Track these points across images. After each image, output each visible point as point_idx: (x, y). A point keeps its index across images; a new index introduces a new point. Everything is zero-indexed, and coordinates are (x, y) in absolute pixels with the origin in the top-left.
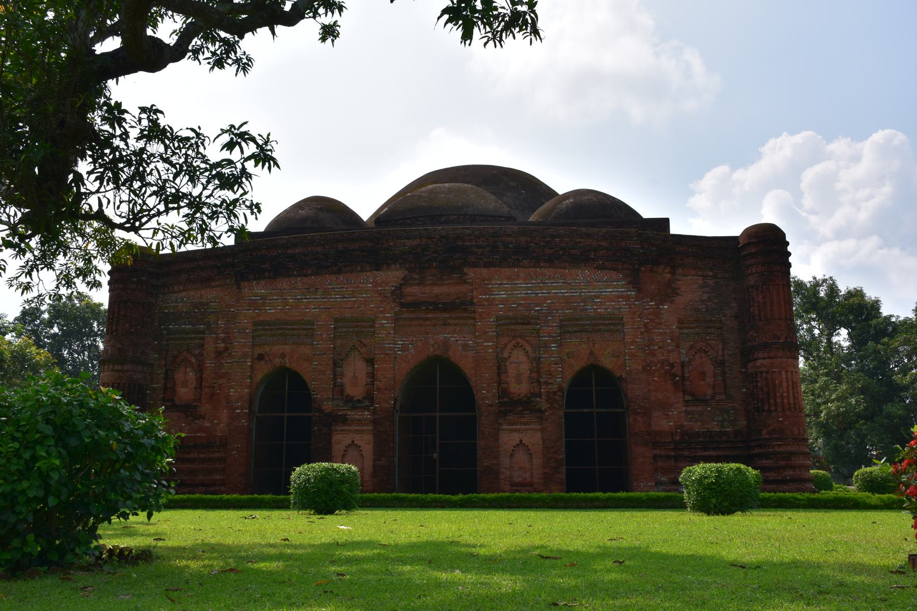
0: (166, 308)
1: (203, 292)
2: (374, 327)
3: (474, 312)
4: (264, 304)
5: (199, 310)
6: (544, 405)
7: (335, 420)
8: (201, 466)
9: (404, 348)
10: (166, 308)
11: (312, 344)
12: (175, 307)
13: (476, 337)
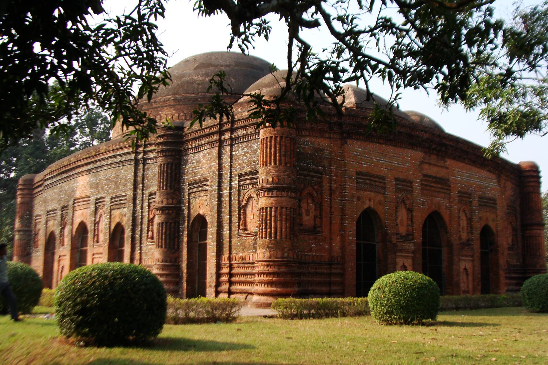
0: (298, 148)
1: (320, 140)
2: (412, 187)
3: (450, 186)
5: (318, 153)
9: (423, 204)
10: (298, 148)
11: (384, 194)
12: (304, 148)
13: (451, 202)
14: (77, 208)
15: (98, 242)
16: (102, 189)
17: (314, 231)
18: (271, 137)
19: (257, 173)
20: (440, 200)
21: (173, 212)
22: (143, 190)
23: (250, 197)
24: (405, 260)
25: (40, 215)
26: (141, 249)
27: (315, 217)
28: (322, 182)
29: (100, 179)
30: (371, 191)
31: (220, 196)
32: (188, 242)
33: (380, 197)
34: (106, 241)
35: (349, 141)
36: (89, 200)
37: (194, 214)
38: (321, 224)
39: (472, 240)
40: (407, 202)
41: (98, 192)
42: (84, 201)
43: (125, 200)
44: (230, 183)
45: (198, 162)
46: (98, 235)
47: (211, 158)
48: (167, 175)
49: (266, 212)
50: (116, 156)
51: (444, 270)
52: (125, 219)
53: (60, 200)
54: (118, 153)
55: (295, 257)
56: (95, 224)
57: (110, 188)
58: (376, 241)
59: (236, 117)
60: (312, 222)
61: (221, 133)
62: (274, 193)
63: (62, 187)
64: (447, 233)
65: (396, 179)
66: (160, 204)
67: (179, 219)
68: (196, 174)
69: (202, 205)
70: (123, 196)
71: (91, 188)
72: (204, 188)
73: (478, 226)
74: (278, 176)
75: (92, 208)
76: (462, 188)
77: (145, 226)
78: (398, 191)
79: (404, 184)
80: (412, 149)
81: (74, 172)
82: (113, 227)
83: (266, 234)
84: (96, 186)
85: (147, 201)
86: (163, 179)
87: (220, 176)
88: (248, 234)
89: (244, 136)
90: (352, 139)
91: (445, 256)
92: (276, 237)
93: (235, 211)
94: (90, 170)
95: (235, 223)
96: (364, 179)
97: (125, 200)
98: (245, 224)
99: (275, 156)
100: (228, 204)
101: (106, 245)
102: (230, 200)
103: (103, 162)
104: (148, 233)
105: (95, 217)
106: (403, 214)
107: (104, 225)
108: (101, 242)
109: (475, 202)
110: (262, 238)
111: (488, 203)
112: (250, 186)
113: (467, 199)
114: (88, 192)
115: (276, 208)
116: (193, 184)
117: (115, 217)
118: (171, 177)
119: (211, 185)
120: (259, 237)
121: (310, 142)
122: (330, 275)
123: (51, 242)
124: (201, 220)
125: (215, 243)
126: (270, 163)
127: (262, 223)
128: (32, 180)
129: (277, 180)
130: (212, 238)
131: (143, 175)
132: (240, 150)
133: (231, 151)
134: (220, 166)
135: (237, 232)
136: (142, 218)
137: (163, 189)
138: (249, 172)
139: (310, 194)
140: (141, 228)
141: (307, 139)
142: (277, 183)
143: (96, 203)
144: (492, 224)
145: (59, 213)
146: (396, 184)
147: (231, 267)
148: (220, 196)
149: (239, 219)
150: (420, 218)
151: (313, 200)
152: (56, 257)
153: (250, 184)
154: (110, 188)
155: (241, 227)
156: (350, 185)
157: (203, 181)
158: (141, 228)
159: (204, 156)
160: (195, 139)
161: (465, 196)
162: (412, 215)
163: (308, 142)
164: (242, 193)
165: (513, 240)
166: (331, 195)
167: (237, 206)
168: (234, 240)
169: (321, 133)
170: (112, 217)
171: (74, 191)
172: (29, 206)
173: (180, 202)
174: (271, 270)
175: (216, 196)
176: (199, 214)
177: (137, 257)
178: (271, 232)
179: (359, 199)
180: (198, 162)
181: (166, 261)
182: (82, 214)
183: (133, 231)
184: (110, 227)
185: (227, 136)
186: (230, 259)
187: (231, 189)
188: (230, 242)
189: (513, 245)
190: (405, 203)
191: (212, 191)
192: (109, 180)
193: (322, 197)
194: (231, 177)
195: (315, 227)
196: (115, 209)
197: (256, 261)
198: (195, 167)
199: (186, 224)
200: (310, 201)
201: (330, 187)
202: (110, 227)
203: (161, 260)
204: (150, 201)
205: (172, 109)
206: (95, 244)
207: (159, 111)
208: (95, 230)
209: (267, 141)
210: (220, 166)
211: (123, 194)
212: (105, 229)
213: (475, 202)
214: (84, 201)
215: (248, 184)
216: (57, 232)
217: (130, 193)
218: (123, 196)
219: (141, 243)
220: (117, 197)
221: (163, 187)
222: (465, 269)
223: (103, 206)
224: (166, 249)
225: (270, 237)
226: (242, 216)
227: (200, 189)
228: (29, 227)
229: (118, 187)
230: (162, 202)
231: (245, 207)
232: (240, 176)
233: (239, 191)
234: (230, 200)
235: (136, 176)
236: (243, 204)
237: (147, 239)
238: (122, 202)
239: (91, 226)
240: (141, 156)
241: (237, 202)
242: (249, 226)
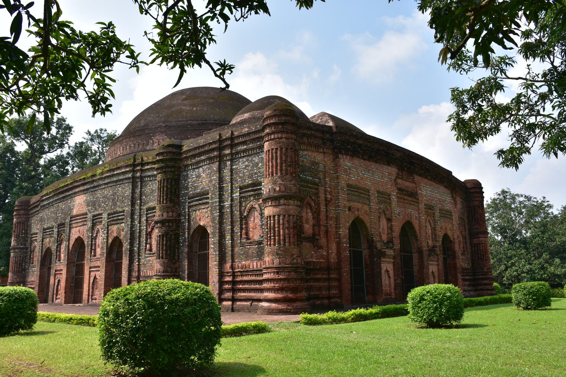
2: (390, 199)
3: (418, 199)
4: (350, 174)
6: (439, 252)
7: (382, 254)
8: (324, 284)
13: (419, 213)
14: (74, 225)
15: (95, 256)
16: (100, 206)
17: (313, 239)
18: (277, 149)
19: (260, 184)
20: (412, 211)
21: (173, 225)
22: (141, 205)
23: (252, 208)
24: (388, 265)
25: (36, 234)
26: (139, 261)
27: (314, 226)
28: (318, 193)
29: (98, 197)
30: (359, 202)
31: (221, 208)
32: (189, 253)
33: (366, 208)
34: (104, 255)
35: (340, 156)
36: (86, 217)
37: (194, 226)
38: (319, 232)
39: (436, 247)
40: (387, 213)
41: (96, 209)
42: (80, 219)
43: (122, 215)
44: (231, 195)
45: (197, 177)
46: (95, 250)
47: (211, 172)
48: (167, 190)
49: (274, 220)
50: (113, 176)
51: (415, 274)
52: (123, 233)
53: (57, 219)
54: (115, 173)
55: (303, 263)
56: (92, 239)
57: (107, 205)
58: (363, 248)
59: (236, 133)
60: (311, 231)
61: (221, 149)
62: (282, 201)
63: (58, 206)
64: (417, 240)
65: (378, 192)
66: (161, 217)
67: (179, 231)
68: (196, 188)
69: (204, 217)
70: (120, 212)
71: (88, 205)
72: (205, 201)
73: (441, 234)
74: (285, 186)
75: (89, 224)
76: (427, 201)
77: (143, 240)
78: (379, 203)
79: (384, 197)
80: (389, 166)
81: (71, 192)
82: (110, 241)
83: (275, 241)
84: (92, 204)
85: (145, 216)
86: (163, 194)
87: (221, 189)
88: (251, 243)
89: (244, 151)
90: (342, 154)
91: (415, 261)
92: (284, 244)
93: (237, 221)
94: (87, 189)
95: (237, 233)
96: (353, 191)
97: (122, 215)
98: (247, 234)
99: (281, 167)
100: (229, 215)
101: (104, 259)
102: (232, 212)
103: (101, 182)
104: (146, 246)
105: (92, 233)
106: (384, 222)
107: (101, 240)
108: (98, 255)
109: (437, 214)
110: (270, 245)
111: (446, 214)
112: (252, 198)
113: (431, 211)
114: (84, 210)
115: (284, 216)
116: (193, 198)
117: (113, 232)
118: (171, 191)
119: (212, 198)
120: (267, 245)
121: (310, 156)
122: (328, 280)
123: (47, 258)
124: (202, 231)
125: (217, 253)
126: (277, 173)
127: (270, 231)
128: (29, 201)
129: (284, 190)
130: (214, 248)
131: (141, 191)
132: (241, 165)
133: (232, 165)
134: (221, 180)
135: (239, 241)
136: (140, 232)
137: (163, 203)
138: (251, 184)
139: (310, 205)
140: (139, 241)
141: (305, 153)
142: (284, 192)
143: (93, 220)
144: (449, 233)
145: (56, 230)
146: (378, 196)
147: (234, 275)
148: (221, 208)
149: (241, 229)
150: (397, 226)
151: (311, 209)
152: (52, 272)
153: (252, 195)
154: (107, 205)
155: (243, 236)
156: (343, 196)
157: (203, 195)
158: (139, 241)
159: (204, 171)
160: (194, 156)
161: (430, 208)
162: (391, 225)
163: (306, 155)
164: (244, 205)
165: (463, 247)
166: (326, 205)
167: (239, 216)
168: (236, 249)
169: (317, 147)
170: (110, 232)
171: (71, 210)
172: (25, 226)
173: (179, 215)
174: (281, 277)
175: (218, 208)
176: (200, 225)
177: (136, 268)
178: (279, 239)
179: (350, 209)
180: (199, 176)
181: (167, 272)
182: (78, 231)
183: (132, 244)
184: (107, 241)
185: (227, 152)
186: (232, 267)
187: (232, 200)
188: (232, 251)
189: (464, 251)
190: (385, 213)
191: (213, 203)
192: (107, 198)
193: (319, 207)
194: (232, 189)
195: (314, 235)
196: (113, 224)
197: (265, 268)
198: (194, 181)
199: (186, 235)
200: (309, 211)
201: (326, 198)
202: (107, 241)
203: (162, 270)
204: (148, 216)
205: (163, 135)
206: (92, 258)
207: (151, 136)
208: (92, 244)
209: (272, 153)
210: (221, 180)
211: (121, 210)
212: (102, 243)
213: (437, 214)
214: (80, 219)
215: (250, 196)
216: (54, 248)
217: (127, 209)
218: (120, 212)
219: (139, 255)
220: (114, 213)
221: (163, 201)
222: (433, 272)
223: (101, 222)
224: (166, 261)
225: (279, 243)
226: (244, 226)
227: (200, 202)
228: (25, 244)
229: (115, 204)
230: (163, 216)
231: (247, 218)
232: (241, 188)
233: (241, 203)
234: (232, 212)
235: (133, 192)
236: (245, 214)
237: (145, 251)
238: (120, 217)
239: (88, 242)
240: (138, 174)
241: (238, 213)
242: (251, 235)
